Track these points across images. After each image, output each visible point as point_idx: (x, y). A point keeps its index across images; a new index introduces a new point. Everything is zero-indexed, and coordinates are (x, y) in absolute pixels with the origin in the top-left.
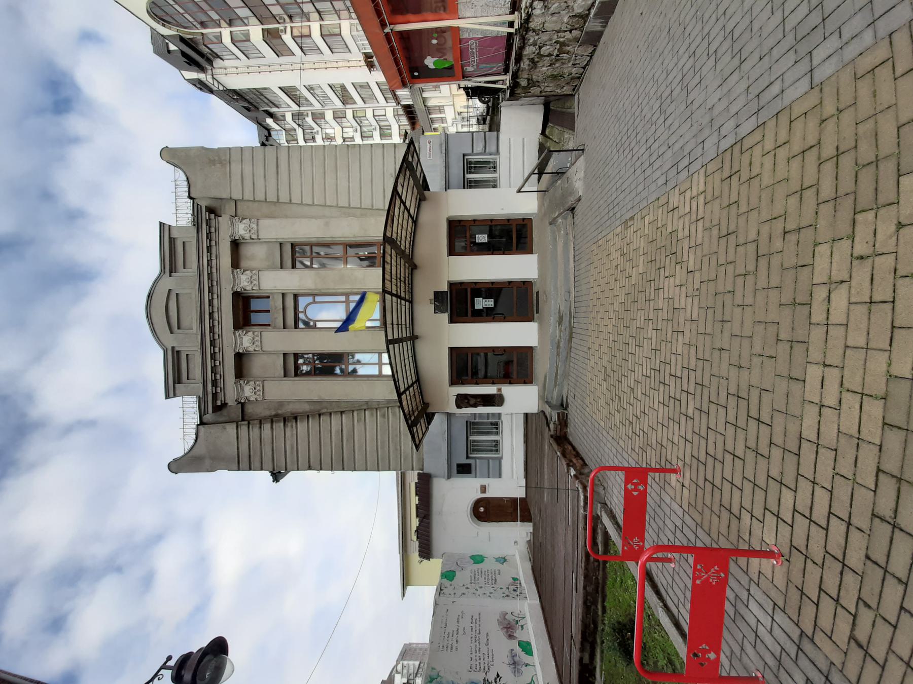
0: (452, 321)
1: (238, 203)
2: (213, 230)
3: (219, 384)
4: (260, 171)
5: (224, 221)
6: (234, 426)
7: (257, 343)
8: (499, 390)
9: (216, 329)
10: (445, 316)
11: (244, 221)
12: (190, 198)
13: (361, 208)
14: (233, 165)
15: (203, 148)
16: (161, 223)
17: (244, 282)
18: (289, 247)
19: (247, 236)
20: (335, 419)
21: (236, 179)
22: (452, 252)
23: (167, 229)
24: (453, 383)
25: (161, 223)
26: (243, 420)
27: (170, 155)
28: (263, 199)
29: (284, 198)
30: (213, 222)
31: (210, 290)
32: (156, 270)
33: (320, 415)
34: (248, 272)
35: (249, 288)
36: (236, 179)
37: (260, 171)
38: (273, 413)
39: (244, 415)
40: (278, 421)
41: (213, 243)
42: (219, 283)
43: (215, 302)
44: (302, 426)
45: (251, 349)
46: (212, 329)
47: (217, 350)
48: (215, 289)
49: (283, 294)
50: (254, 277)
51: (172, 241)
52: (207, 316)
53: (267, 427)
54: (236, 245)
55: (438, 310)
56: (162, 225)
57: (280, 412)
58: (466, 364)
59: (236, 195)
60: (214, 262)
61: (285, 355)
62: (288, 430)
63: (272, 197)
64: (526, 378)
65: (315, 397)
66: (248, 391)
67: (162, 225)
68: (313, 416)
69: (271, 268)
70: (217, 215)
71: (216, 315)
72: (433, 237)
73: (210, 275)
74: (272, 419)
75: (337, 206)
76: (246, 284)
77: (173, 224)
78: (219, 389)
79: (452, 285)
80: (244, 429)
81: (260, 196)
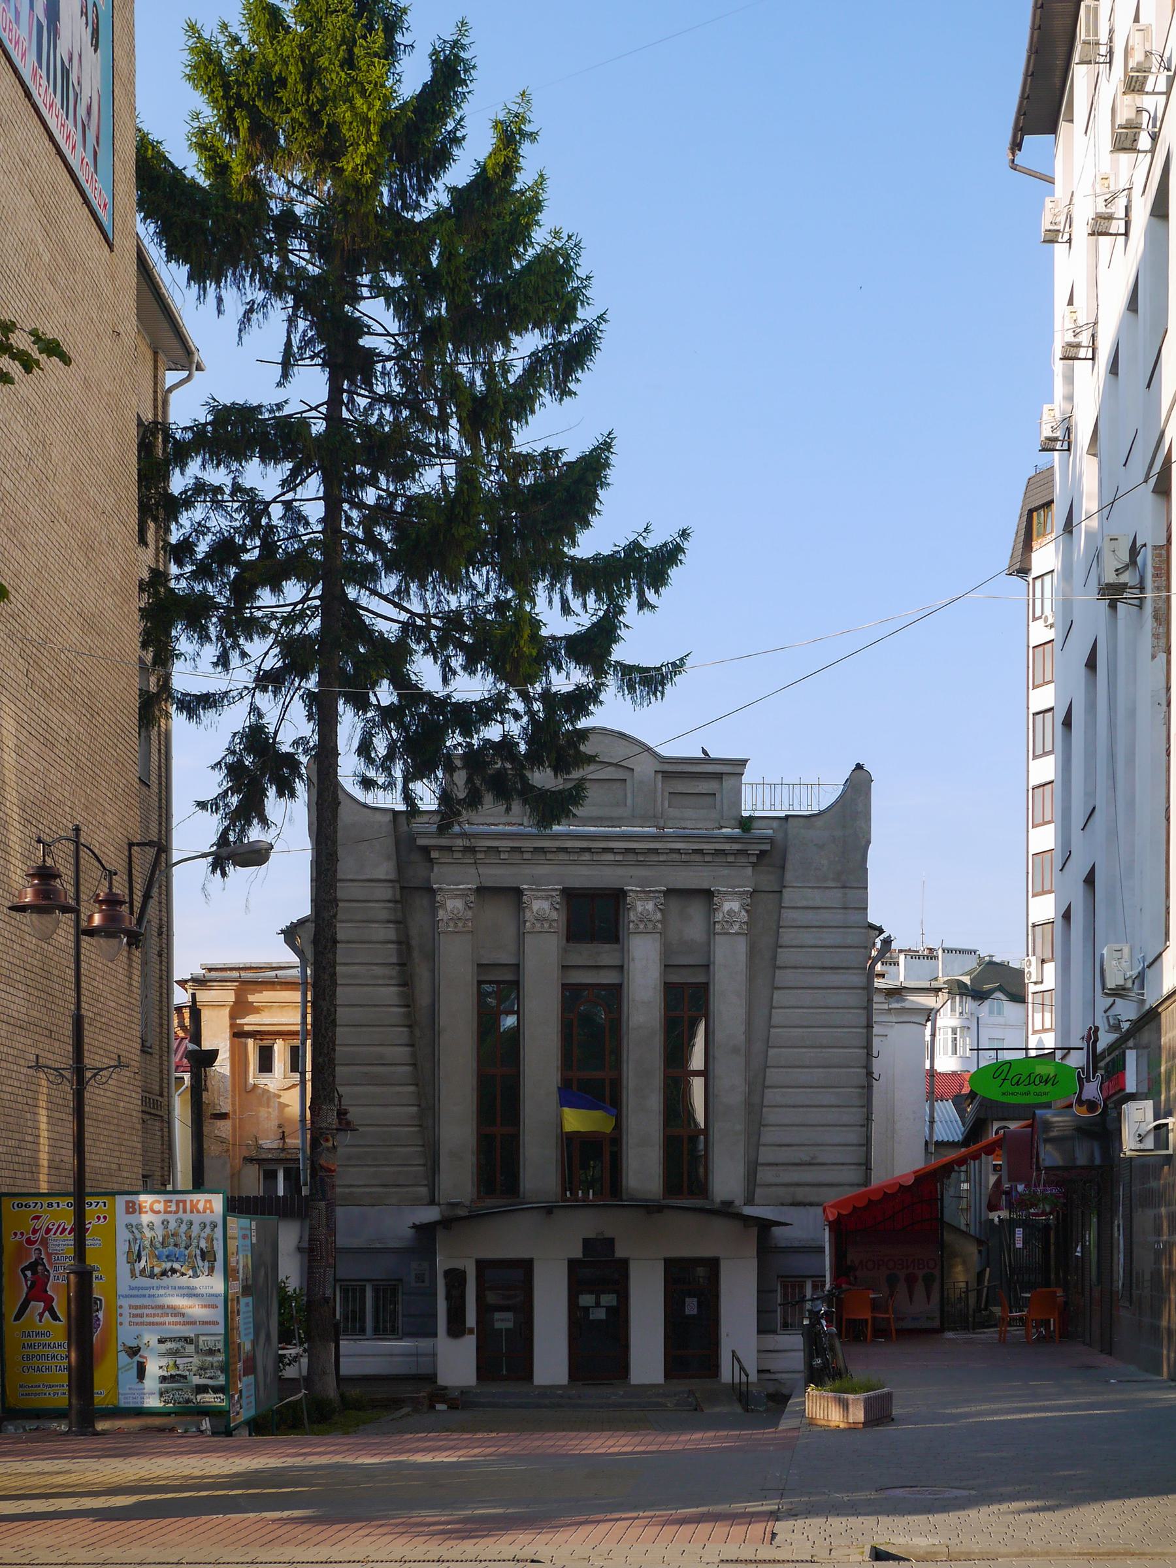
0: (573, 1264)
1: (777, 895)
2: (731, 859)
3: (468, 855)
4: (829, 938)
5: (745, 878)
6: (392, 876)
7: (538, 925)
8: (471, 1331)
9: (563, 856)
10: (578, 1253)
11: (743, 913)
12: (787, 817)
13: (762, 1106)
14: (838, 893)
15: (869, 842)
16: (746, 761)
17: (643, 907)
18: (701, 979)
19: (719, 917)
20: (401, 1053)
21: (816, 898)
22: (669, 1263)
23: (737, 770)
24: (481, 1265)
25: (746, 761)
26: (402, 888)
27: (859, 783)
28: (782, 942)
29: (783, 977)
30: (743, 859)
31: (628, 851)
32: (664, 751)
33: (409, 1026)
34: (659, 916)
35: (632, 916)
36: (816, 898)
37: (829, 938)
38: (414, 943)
39: (412, 893)
40: (400, 953)
41: (708, 858)
42: (639, 863)
43: (610, 857)
44: (389, 993)
45: (528, 914)
46: (565, 850)
47: (527, 856)
48: (631, 857)
49: (622, 967)
50: (650, 926)
51: (719, 776)
52: (584, 844)
53: (390, 933)
54: (708, 894)
55: (586, 1242)
56: (743, 763)
57: (416, 954)
58: (510, 1282)
59: (790, 896)
60: (676, 857)
61: (518, 965)
62: (387, 971)
63: (784, 956)
64: (486, 1369)
65: (444, 1020)
66: (454, 905)
67: (743, 763)
68: (408, 1015)
69: (667, 950)
70: (754, 865)
71: (587, 856)
72: (692, 1240)
73: (655, 851)
74: (404, 944)
75: (766, 1067)
76: (640, 909)
77: (745, 779)
78: (459, 855)
79: (625, 1263)
80: (386, 892)
81: (787, 937)
